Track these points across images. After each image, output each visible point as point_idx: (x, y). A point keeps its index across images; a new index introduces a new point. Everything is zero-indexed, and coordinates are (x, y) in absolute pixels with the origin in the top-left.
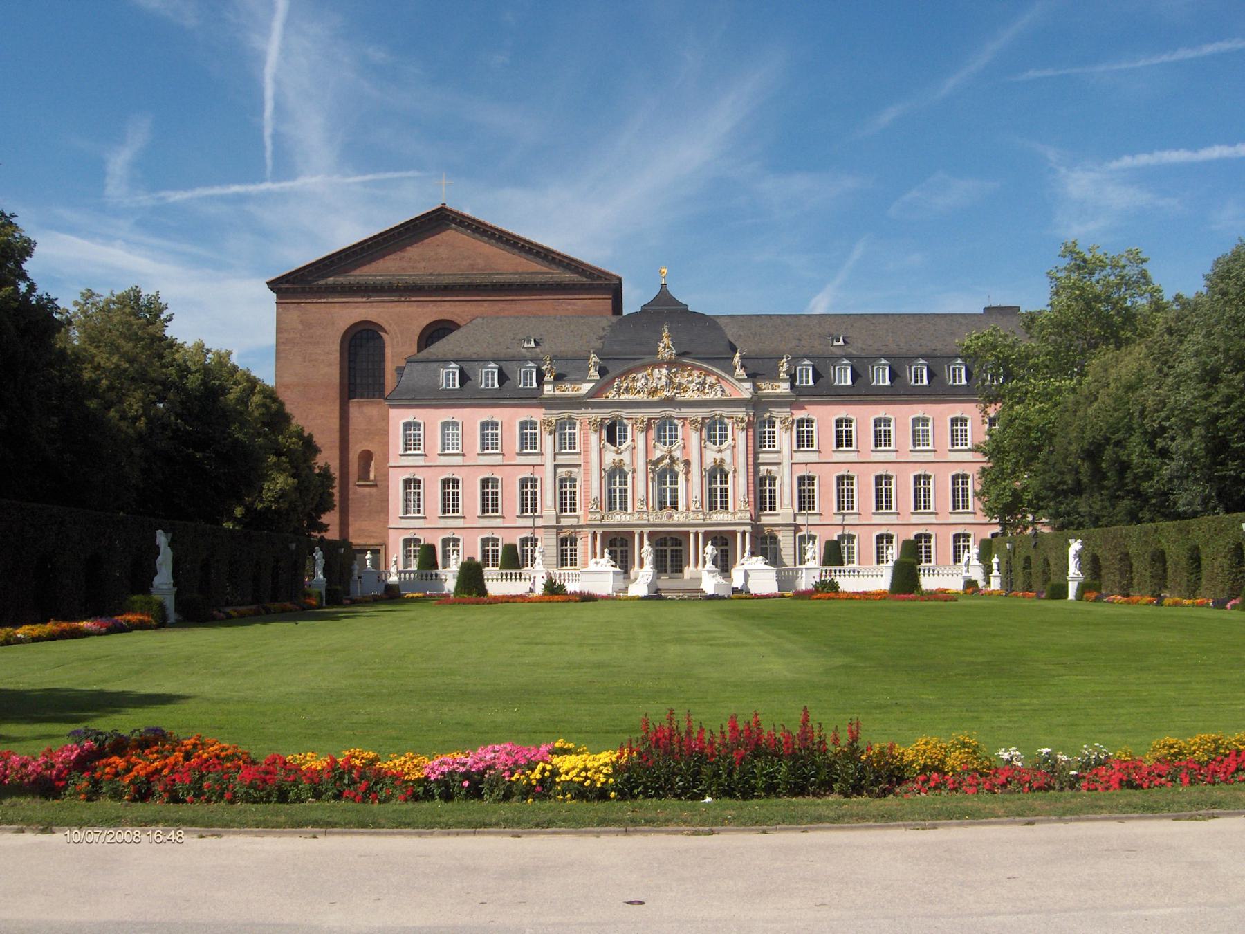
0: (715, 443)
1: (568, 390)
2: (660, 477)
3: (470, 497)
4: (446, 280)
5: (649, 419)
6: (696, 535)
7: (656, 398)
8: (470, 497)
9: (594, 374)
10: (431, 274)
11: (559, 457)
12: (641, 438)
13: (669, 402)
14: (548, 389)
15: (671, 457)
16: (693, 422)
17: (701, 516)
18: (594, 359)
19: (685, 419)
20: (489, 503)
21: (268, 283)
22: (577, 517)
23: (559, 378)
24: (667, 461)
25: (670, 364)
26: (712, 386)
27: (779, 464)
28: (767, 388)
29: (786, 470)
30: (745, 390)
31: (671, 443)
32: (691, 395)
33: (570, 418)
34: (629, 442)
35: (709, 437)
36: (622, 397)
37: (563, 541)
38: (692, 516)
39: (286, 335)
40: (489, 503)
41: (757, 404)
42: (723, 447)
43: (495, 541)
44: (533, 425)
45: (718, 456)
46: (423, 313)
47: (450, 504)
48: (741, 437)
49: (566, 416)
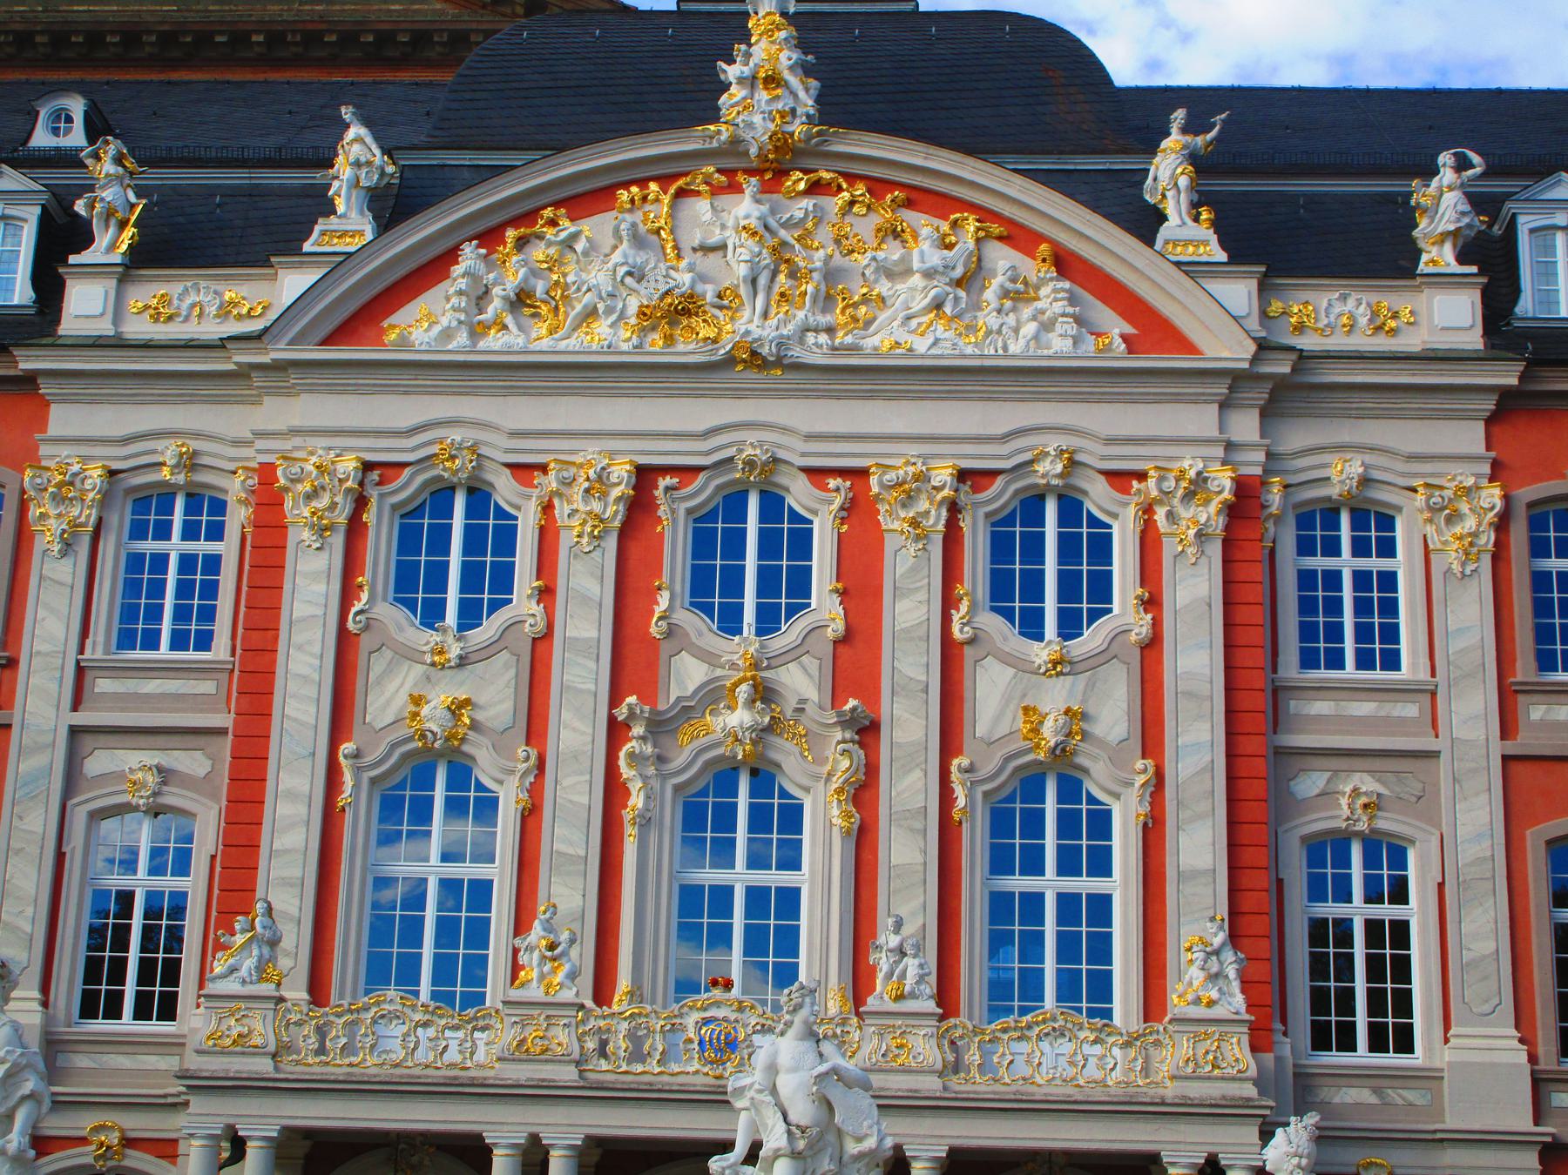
0: (1032, 626)
2: (693, 817)
5: (645, 475)
7: (687, 349)
9: (348, 224)
11: (104, 685)
12: (588, 580)
15: (764, 694)
17: (925, 1047)
18: (358, 153)
22: (174, 1045)
23: (161, 248)
24: (739, 718)
25: (775, 167)
26: (1018, 295)
27: (1435, 755)
28: (1336, 315)
30: (1221, 315)
31: (768, 621)
33: (190, 462)
34: (523, 603)
35: (1000, 590)
41: (1286, 386)
48: (1195, 586)
49: (169, 451)
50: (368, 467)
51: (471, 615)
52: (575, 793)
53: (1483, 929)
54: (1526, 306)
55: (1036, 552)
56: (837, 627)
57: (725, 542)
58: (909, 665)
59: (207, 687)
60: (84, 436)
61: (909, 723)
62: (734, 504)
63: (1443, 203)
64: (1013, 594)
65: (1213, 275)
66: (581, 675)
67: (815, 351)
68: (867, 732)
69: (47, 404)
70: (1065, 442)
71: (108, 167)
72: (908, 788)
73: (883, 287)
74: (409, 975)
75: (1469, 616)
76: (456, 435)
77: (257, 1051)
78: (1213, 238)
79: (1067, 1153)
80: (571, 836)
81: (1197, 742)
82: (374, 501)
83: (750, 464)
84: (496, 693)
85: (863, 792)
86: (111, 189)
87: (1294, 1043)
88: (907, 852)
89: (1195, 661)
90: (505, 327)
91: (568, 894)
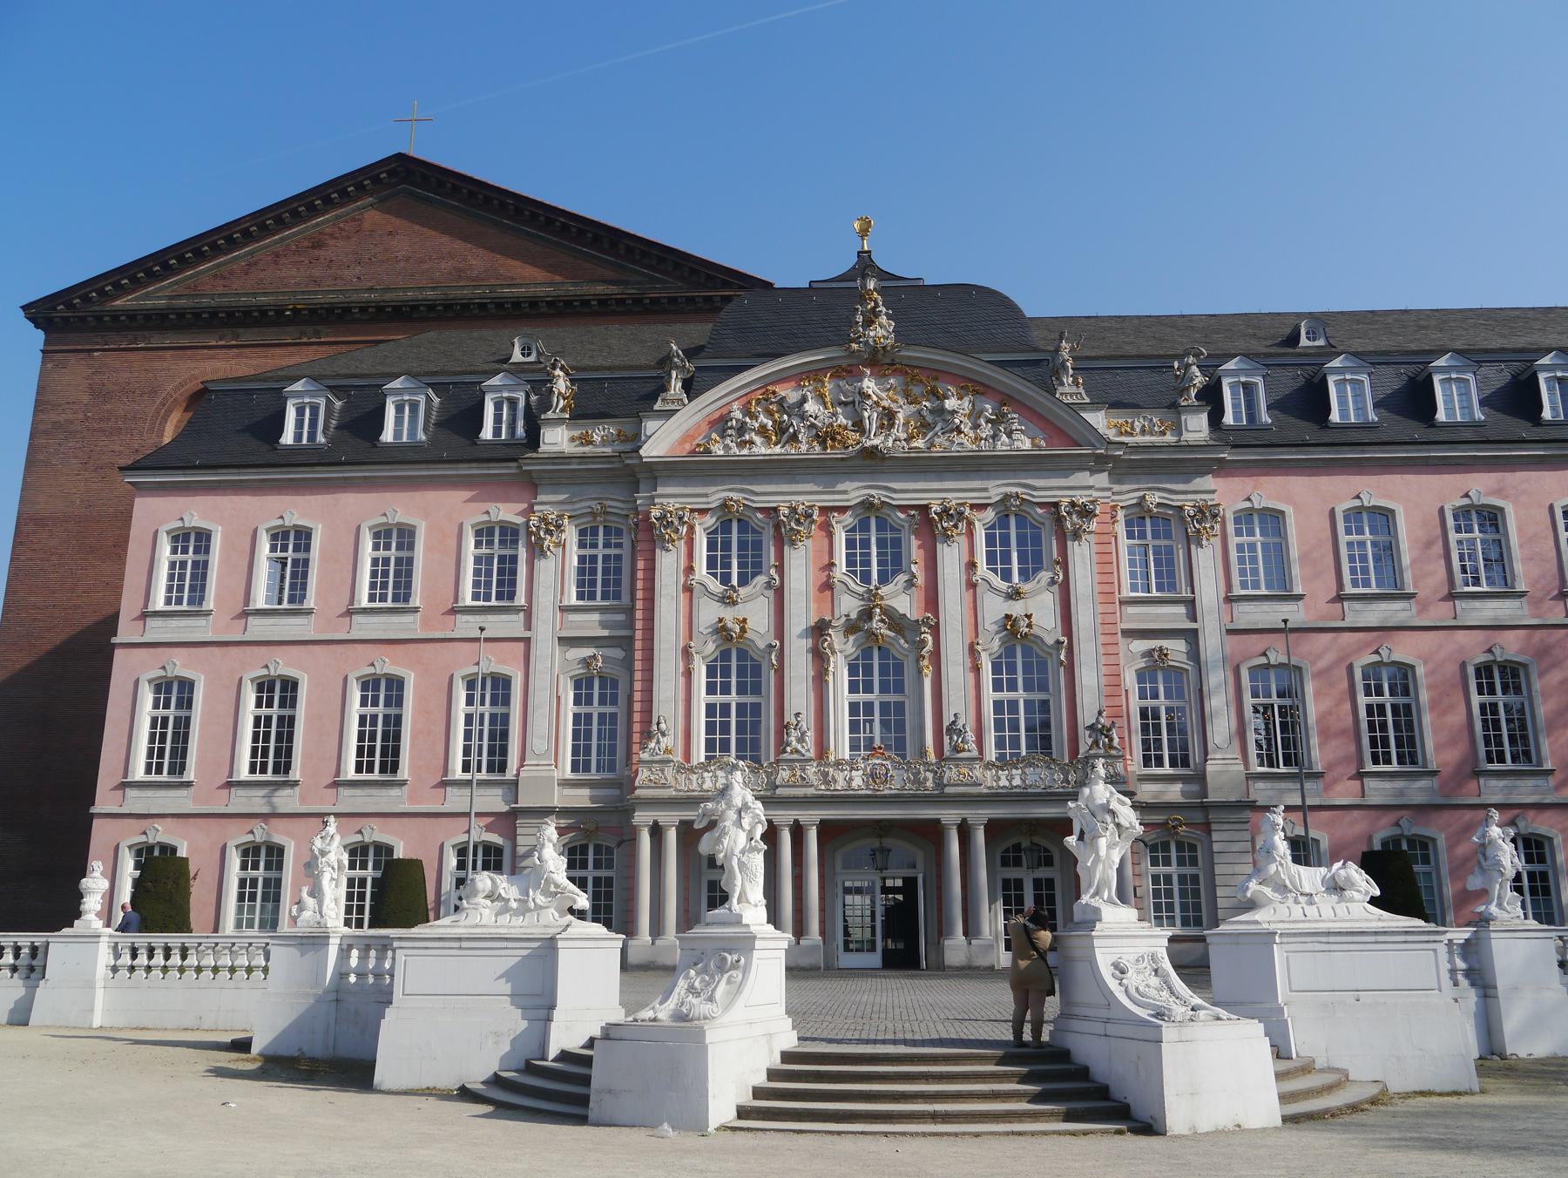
0: (1006, 576)
3: (330, 728)
6: (965, 830)
10: (371, 290)
13: (872, 461)
16: (945, 512)
19: (925, 509)
20: (382, 750)
21: (24, 308)
25: (879, 361)
27: (1195, 631)
31: (884, 579)
36: (745, 452)
38: (951, 774)
39: (54, 418)
40: (382, 750)
42: (1026, 587)
43: (383, 850)
44: (509, 533)
45: (1017, 609)
47: (275, 749)
50: (692, 511)
51: (743, 581)
54: (1228, 419)
56: (920, 580)
59: (621, 617)
62: (864, 526)
65: (1084, 410)
67: (901, 449)
68: (935, 630)
69: (536, 486)
70: (1020, 490)
71: (558, 372)
73: (929, 419)
74: (725, 747)
76: (731, 495)
77: (664, 786)
78: (1081, 390)
79: (1037, 820)
82: (697, 528)
83: (872, 504)
85: (936, 655)
86: (561, 385)
90: (752, 442)
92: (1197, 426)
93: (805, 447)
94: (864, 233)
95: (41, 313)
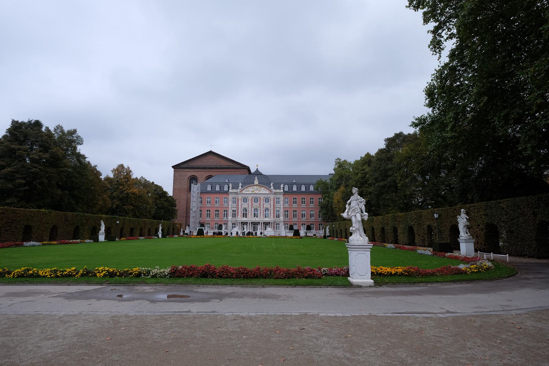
1: (235, 191)
3: (213, 213)
4: (211, 167)
8: (213, 213)
9: (240, 187)
12: (250, 202)
14: (230, 191)
18: (240, 184)
25: (256, 185)
28: (278, 191)
29: (282, 210)
32: (261, 192)
37: (233, 224)
46: (206, 174)
47: (208, 215)
48: (272, 202)
52: (250, 210)
53: (282, 214)
55: (267, 200)
57: (256, 200)
58: (262, 205)
60: (230, 197)
61: (262, 207)
63: (282, 186)
64: (266, 202)
66: (250, 205)
72: (262, 209)
75: (282, 202)
80: (250, 211)
81: (272, 207)
84: (247, 206)
87: (275, 218)
88: (262, 211)
89: (272, 204)
91: (250, 213)
92: (282, 191)
93: (251, 192)
94: (257, 166)
95: (173, 167)
